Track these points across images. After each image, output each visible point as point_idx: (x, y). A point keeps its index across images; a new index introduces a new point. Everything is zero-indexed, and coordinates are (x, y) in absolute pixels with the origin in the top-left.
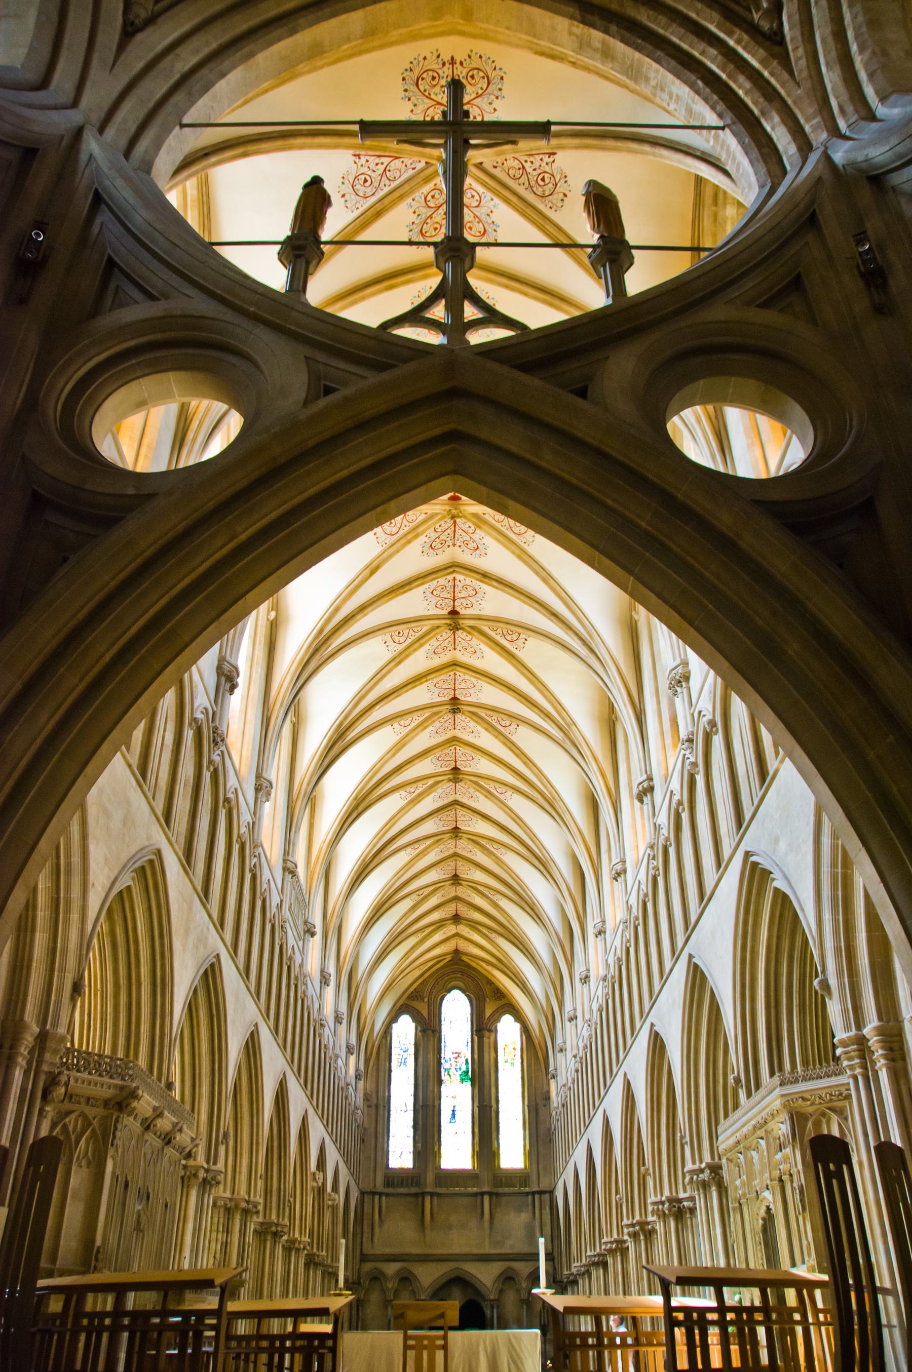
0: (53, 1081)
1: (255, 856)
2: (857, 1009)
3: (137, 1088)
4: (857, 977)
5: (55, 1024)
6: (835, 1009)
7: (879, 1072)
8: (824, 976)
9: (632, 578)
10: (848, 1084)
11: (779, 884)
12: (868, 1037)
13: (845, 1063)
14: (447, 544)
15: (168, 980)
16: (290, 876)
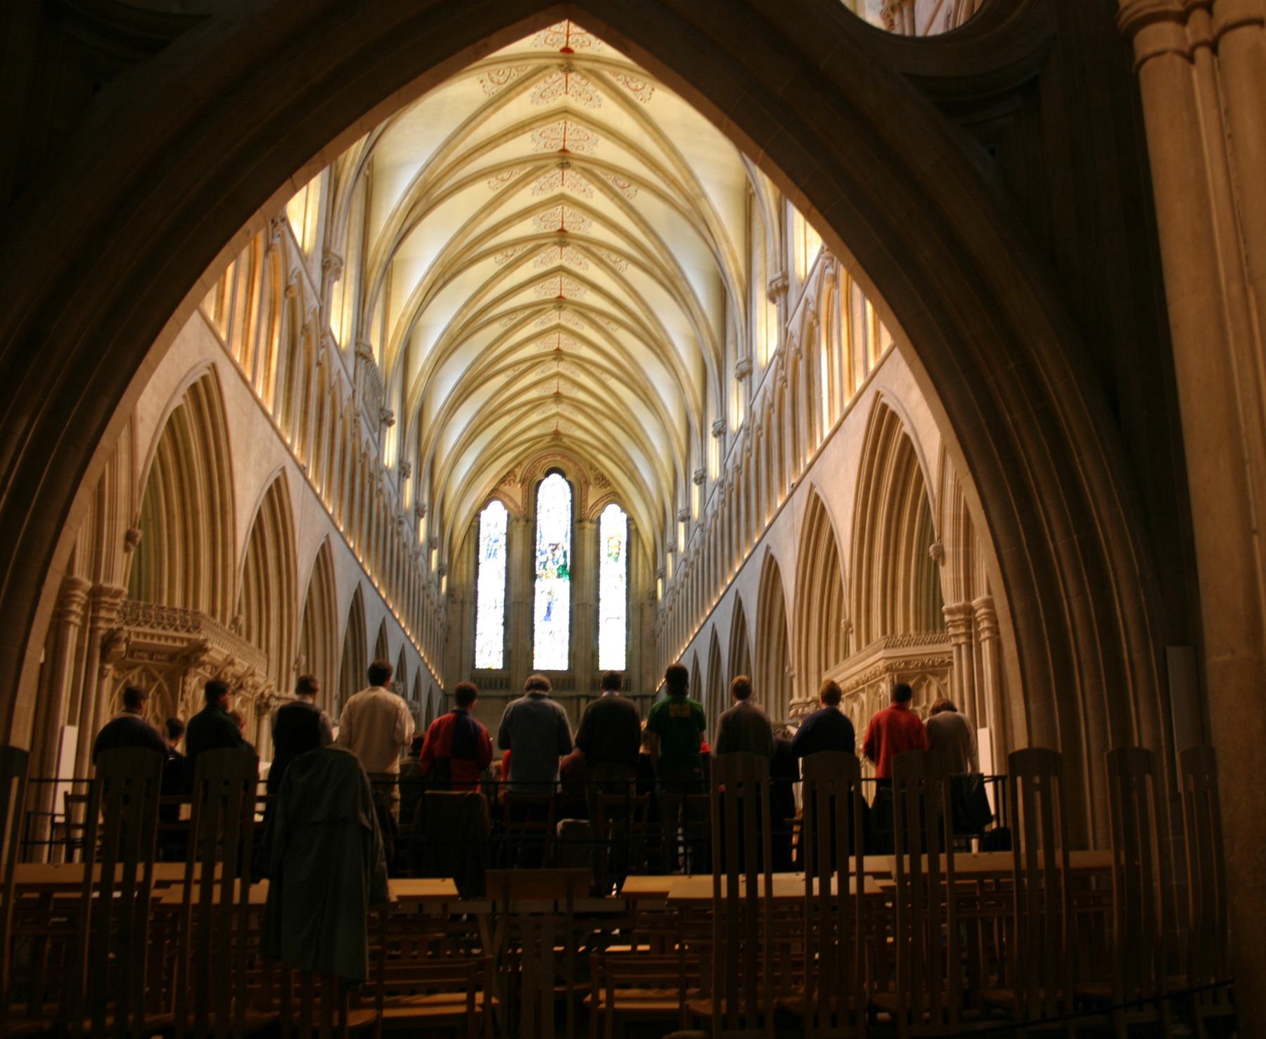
0: (111, 639)
1: (323, 347)
2: (969, 579)
3: (205, 640)
4: (972, 546)
5: (109, 578)
6: (947, 576)
7: (983, 644)
8: (940, 542)
9: (762, 152)
10: (951, 652)
11: (907, 429)
12: (976, 608)
13: (951, 631)
14: (558, 93)
15: (229, 506)
16: (364, 362)
